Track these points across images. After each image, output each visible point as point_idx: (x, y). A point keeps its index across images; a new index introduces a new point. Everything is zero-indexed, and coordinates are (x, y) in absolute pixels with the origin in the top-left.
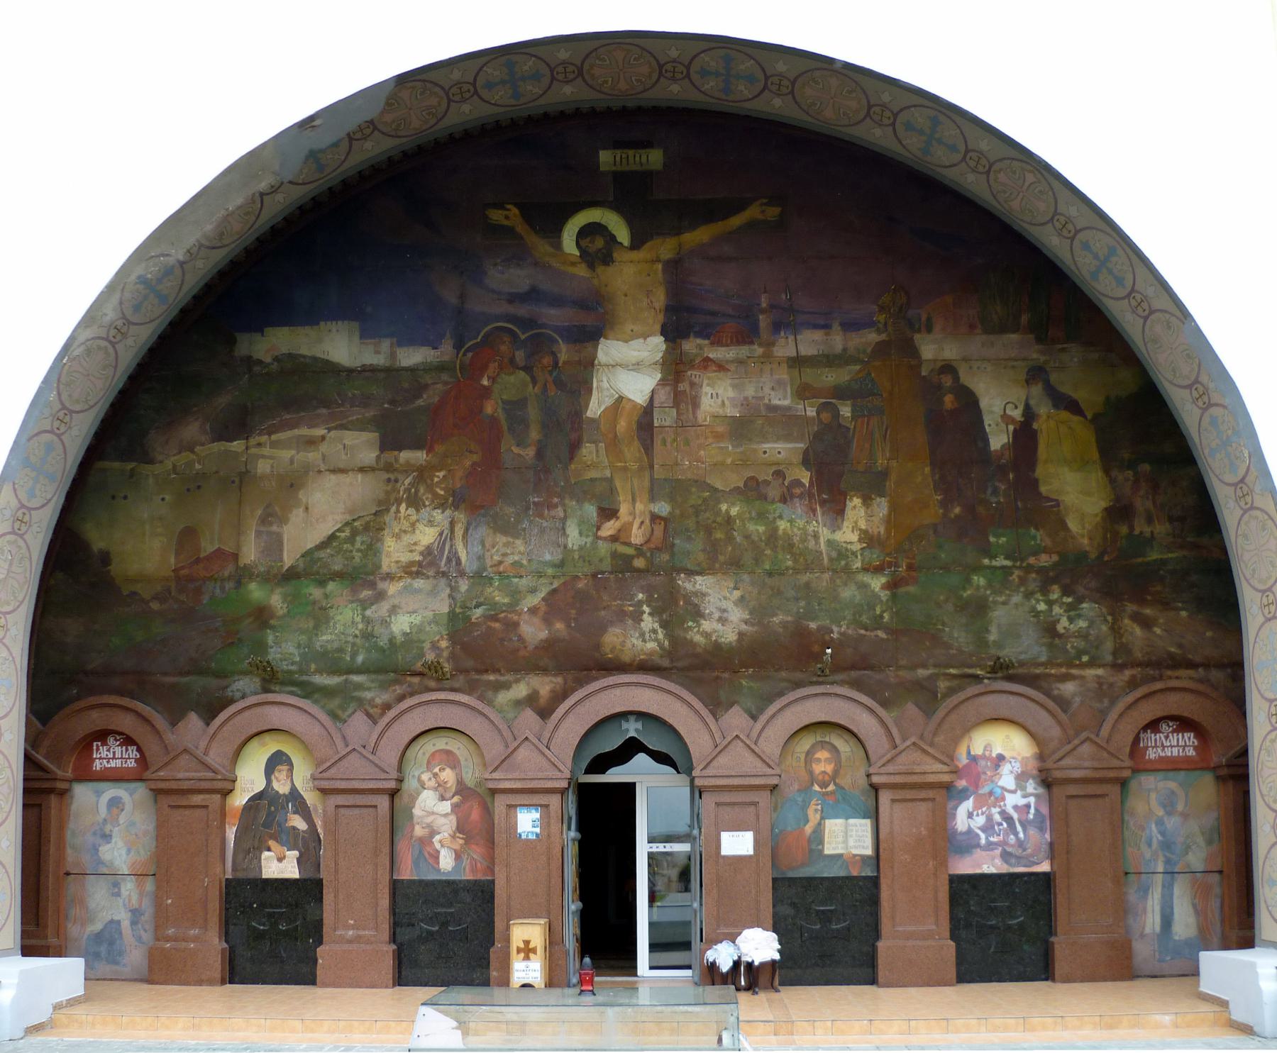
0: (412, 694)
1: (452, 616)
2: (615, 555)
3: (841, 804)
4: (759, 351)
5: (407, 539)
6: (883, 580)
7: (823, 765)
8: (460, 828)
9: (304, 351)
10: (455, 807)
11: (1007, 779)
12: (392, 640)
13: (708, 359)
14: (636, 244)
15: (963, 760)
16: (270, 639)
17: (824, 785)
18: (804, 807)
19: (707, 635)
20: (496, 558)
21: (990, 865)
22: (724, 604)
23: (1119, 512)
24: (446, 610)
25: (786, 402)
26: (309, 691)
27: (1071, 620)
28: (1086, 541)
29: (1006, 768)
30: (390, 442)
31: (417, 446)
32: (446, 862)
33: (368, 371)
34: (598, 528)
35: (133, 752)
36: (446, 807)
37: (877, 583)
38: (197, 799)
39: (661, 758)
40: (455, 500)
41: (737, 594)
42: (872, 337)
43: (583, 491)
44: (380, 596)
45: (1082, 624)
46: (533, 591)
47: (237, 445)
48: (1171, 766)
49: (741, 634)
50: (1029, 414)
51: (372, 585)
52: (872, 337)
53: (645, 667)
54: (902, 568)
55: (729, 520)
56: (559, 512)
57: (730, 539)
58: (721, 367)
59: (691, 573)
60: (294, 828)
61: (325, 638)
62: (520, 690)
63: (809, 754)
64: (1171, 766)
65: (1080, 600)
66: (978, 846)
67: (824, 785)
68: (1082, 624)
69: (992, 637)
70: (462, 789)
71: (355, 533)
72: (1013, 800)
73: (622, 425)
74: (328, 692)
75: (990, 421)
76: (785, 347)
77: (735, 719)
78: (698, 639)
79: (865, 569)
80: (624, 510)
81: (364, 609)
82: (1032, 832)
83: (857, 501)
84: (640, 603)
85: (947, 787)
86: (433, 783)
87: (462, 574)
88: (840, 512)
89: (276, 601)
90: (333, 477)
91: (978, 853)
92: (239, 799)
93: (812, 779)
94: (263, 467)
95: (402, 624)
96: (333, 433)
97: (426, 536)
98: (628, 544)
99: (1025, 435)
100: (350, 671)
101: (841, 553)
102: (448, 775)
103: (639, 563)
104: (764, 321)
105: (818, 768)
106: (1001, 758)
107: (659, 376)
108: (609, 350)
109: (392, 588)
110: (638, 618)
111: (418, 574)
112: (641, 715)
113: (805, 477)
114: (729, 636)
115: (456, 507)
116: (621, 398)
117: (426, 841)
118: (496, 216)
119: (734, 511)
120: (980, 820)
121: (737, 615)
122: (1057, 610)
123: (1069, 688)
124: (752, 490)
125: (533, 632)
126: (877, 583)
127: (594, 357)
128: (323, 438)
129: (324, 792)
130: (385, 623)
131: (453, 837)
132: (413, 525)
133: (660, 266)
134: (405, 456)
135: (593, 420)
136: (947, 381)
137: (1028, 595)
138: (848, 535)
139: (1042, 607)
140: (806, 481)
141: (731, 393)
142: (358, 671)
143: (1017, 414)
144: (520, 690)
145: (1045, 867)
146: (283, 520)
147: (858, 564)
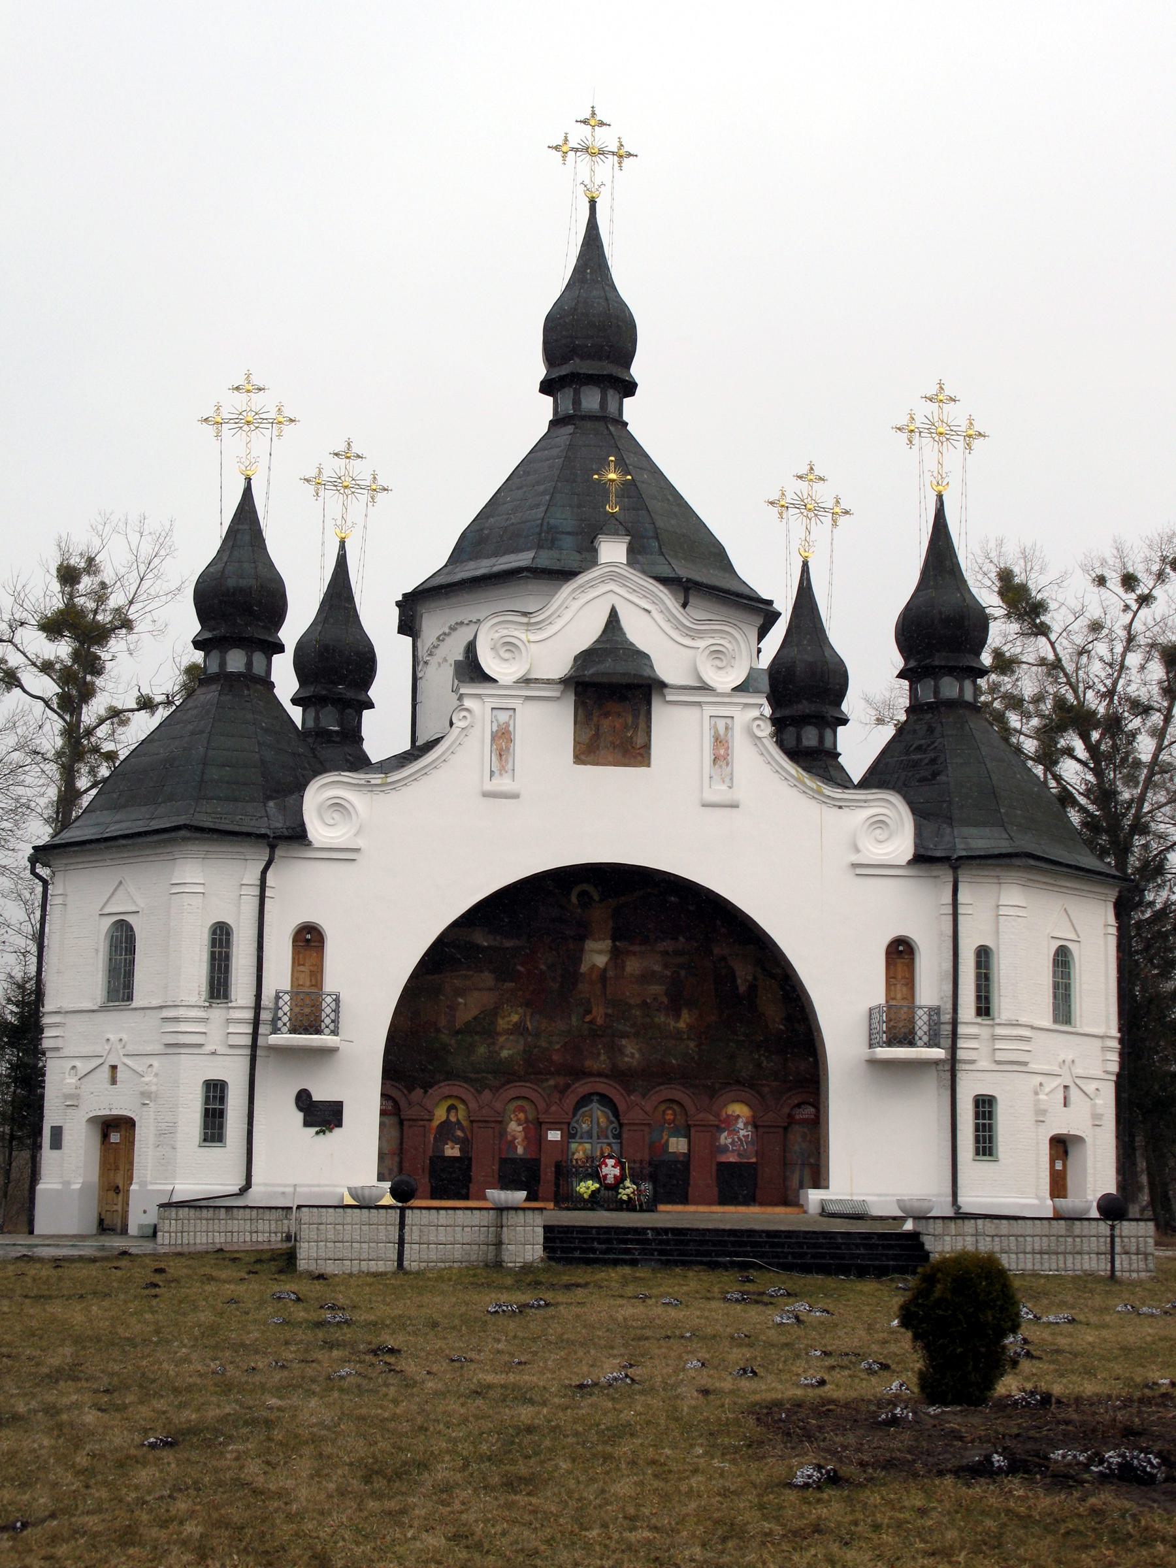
0: (509, 1083)
1: (525, 1051)
3: (676, 1133)
4: (649, 948)
5: (507, 1019)
7: (669, 1116)
8: (526, 1138)
11: (740, 1125)
14: (601, 901)
15: (724, 1115)
17: (670, 1124)
21: (732, 1159)
22: (633, 1051)
26: (467, 1080)
29: (740, 1120)
36: (520, 1128)
37: (692, 1044)
38: (421, 1123)
40: (528, 1004)
46: (558, 1043)
47: (435, 976)
50: (755, 978)
53: (600, 1074)
58: (634, 954)
62: (552, 1082)
63: (664, 1112)
66: (728, 1150)
67: (670, 1124)
70: (527, 1121)
72: (742, 1133)
73: (594, 977)
82: (750, 1146)
85: (717, 1127)
91: (729, 1154)
92: (436, 1123)
95: (505, 1053)
97: (515, 1018)
99: (753, 988)
101: (679, 1031)
102: (522, 1116)
105: (667, 1117)
106: (738, 1116)
108: (590, 945)
110: (599, 1054)
113: (665, 1000)
116: (594, 965)
119: (638, 1013)
120: (730, 1140)
122: (762, 1058)
123: (766, 1090)
126: (692, 1044)
129: (472, 1122)
130: (499, 1054)
131: (523, 1141)
135: (582, 974)
138: (682, 1025)
143: (750, 978)
144: (552, 1082)
145: (754, 1160)
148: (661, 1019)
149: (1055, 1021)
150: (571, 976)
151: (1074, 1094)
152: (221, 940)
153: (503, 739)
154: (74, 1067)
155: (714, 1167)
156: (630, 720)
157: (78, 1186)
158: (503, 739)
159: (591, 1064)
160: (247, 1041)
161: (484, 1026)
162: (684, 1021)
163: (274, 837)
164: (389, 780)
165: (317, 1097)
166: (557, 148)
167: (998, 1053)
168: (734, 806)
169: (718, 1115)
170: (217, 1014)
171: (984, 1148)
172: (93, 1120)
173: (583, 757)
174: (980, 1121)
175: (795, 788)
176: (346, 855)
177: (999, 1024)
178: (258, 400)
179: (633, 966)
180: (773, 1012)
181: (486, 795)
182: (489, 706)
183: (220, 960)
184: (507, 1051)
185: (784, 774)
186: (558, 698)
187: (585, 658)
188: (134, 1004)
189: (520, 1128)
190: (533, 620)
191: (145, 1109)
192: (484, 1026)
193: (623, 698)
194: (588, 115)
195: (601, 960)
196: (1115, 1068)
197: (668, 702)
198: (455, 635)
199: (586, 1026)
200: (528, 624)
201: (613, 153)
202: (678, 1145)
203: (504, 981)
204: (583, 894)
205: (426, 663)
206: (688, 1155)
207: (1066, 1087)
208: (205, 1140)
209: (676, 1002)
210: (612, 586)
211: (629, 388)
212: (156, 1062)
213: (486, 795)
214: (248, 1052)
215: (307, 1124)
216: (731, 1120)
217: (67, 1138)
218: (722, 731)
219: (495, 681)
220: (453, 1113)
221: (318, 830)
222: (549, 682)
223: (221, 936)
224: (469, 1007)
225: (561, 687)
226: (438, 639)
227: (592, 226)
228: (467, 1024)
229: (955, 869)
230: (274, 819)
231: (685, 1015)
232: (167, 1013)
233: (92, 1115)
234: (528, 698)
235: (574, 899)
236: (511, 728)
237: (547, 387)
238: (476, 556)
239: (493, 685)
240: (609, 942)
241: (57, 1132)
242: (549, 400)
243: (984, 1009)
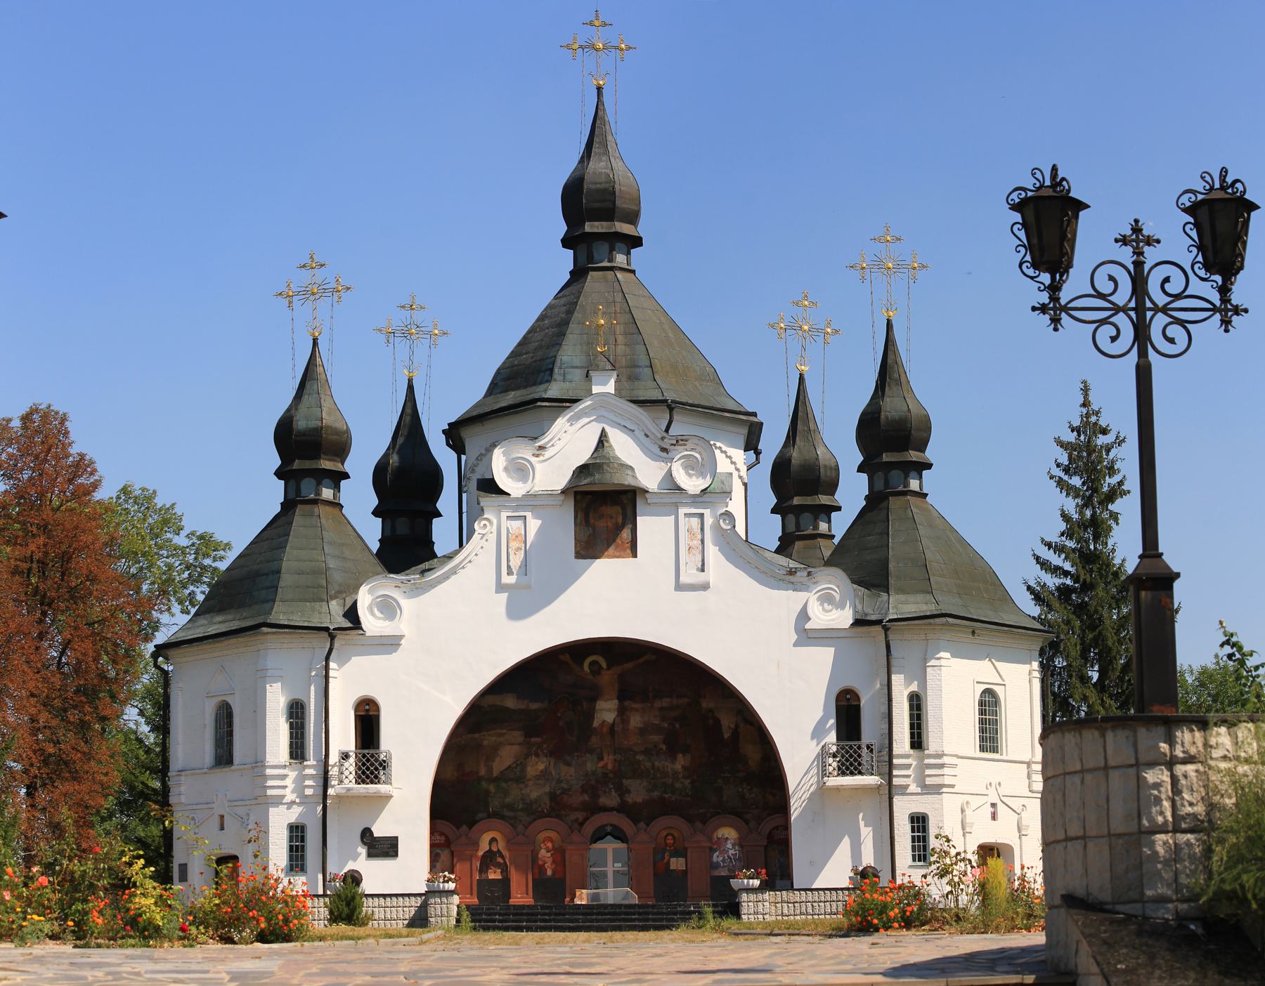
4: (649, 705)
6: (689, 781)
8: (554, 862)
9: (498, 704)
10: (552, 855)
14: (608, 669)
16: (490, 800)
25: (657, 722)
26: (502, 817)
29: (729, 842)
35: (443, 838)
36: (549, 854)
37: (687, 782)
39: (616, 838)
42: (686, 700)
43: (591, 751)
44: (526, 786)
45: (753, 795)
47: (477, 735)
50: (737, 726)
52: (686, 700)
53: (612, 809)
54: (695, 777)
58: (637, 710)
59: (627, 779)
61: (508, 800)
71: (517, 765)
72: (731, 852)
73: (605, 729)
75: (724, 729)
76: (658, 704)
77: (642, 825)
80: (605, 758)
83: (681, 755)
84: (611, 789)
88: (676, 759)
89: (492, 788)
90: (509, 747)
92: (481, 853)
93: (666, 845)
94: (485, 743)
95: (534, 795)
97: (541, 767)
99: (735, 733)
102: (550, 845)
106: (727, 838)
107: (616, 713)
108: (601, 704)
109: (531, 783)
111: (538, 779)
112: (611, 825)
113: (664, 747)
114: (639, 800)
115: (551, 756)
116: (604, 721)
118: (561, 657)
124: (647, 752)
134: (533, 740)
135: (595, 728)
143: (733, 726)
146: (494, 761)
147: (681, 776)
149: (982, 749)
151: (1001, 809)
152: (297, 713)
156: (620, 520)
159: (604, 800)
161: (516, 775)
162: (680, 762)
163: (334, 629)
165: (377, 833)
168: (705, 587)
169: (710, 838)
171: (919, 855)
173: (583, 552)
174: (916, 834)
177: (930, 756)
178: (320, 275)
179: (636, 721)
180: (752, 754)
183: (297, 728)
184: (535, 793)
189: (549, 854)
192: (516, 775)
195: (610, 717)
196: (1039, 786)
202: (677, 864)
203: (664, 743)
204: (593, 663)
206: (685, 872)
207: (993, 805)
208: (291, 870)
211: (637, 242)
219: (509, 495)
221: (372, 623)
222: (550, 495)
224: (506, 757)
225: (562, 497)
226: (477, 459)
228: (501, 772)
229: (886, 629)
230: (334, 614)
237: (567, 242)
238: (506, 391)
240: (616, 701)
241: (183, 868)
242: (570, 253)
243: (917, 742)
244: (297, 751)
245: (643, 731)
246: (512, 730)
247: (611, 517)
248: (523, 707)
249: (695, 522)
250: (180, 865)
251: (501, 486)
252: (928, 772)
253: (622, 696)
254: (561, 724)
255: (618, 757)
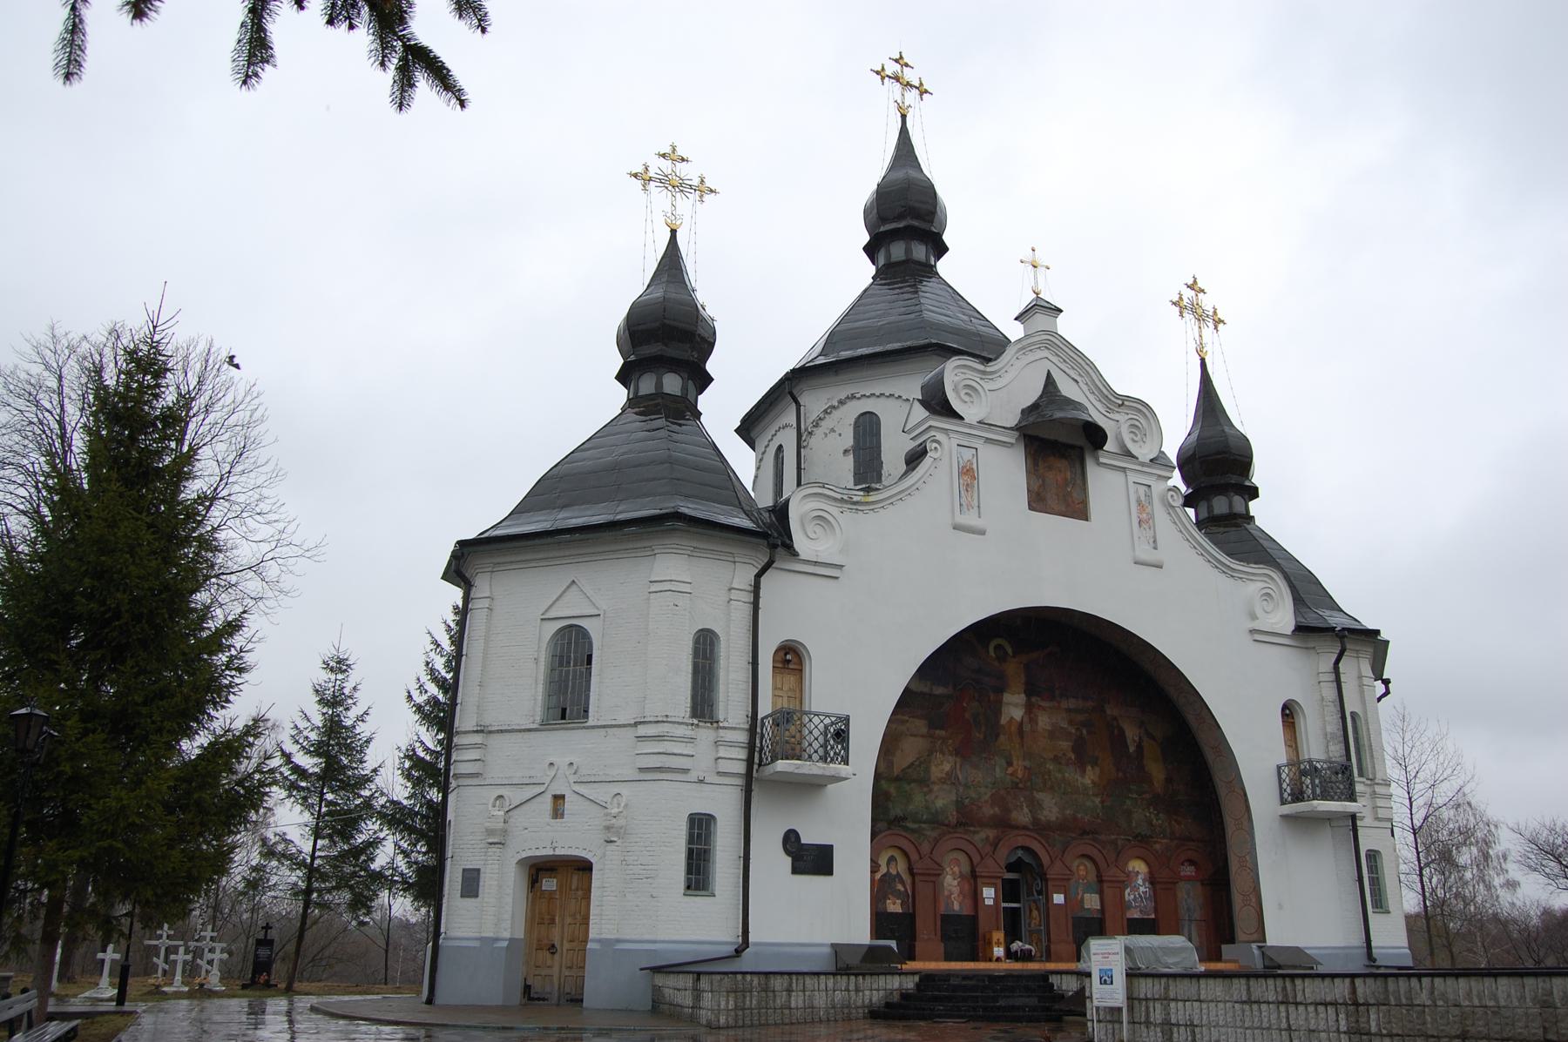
1: (957, 801)
2: (1013, 782)
3: (1088, 890)
8: (961, 892)
10: (959, 883)
12: (936, 811)
13: (1040, 706)
16: (891, 805)
18: (1077, 888)
19: (1046, 817)
20: (972, 779)
21: (1137, 915)
23: (1169, 780)
24: (955, 799)
27: (1157, 820)
28: (1159, 790)
29: (1140, 877)
30: (932, 725)
31: (942, 728)
32: (956, 907)
33: (923, 694)
34: (1007, 770)
36: (956, 883)
37: (1097, 800)
40: (957, 753)
41: (1054, 801)
46: (986, 794)
48: (1188, 879)
49: (1057, 818)
51: (928, 786)
53: (1025, 828)
55: (1050, 771)
56: (993, 762)
57: (1050, 779)
58: (1044, 709)
60: (899, 890)
63: (1078, 866)
64: (1188, 879)
65: (1159, 813)
68: (1160, 822)
69: (1134, 825)
72: (1142, 889)
74: (913, 831)
76: (1064, 704)
78: (1043, 818)
79: (1093, 795)
80: (1015, 763)
81: (925, 796)
82: (1149, 902)
86: (951, 873)
87: (960, 784)
88: (1085, 771)
89: (893, 791)
90: (912, 738)
95: (939, 803)
96: (911, 719)
97: (947, 767)
98: (1017, 778)
99: (1139, 747)
100: (921, 822)
102: (956, 869)
103: (1020, 785)
104: (1057, 692)
105: (1081, 873)
108: (1007, 697)
109: (936, 788)
111: (944, 783)
115: (956, 755)
117: (949, 897)
119: (1051, 767)
120: (1132, 897)
121: (1055, 810)
122: (1153, 816)
124: (1056, 759)
125: (989, 811)
127: (1002, 699)
128: (907, 721)
132: (942, 761)
133: (1022, 666)
134: (937, 732)
136: (1115, 723)
137: (1143, 810)
139: (1148, 814)
140: (1073, 757)
141: (1048, 720)
142: (924, 823)
143: (1137, 739)
144: (982, 835)
145: (1153, 916)
148: (1071, 774)
150: (994, 728)
152: (705, 651)
153: (968, 473)
154: (501, 797)
155: (1125, 923)
157: (505, 944)
158: (968, 473)
160: (741, 768)
162: (1089, 777)
164: (871, 499)
166: (878, 73)
167: (1379, 810)
170: (705, 734)
172: (521, 862)
173: (1034, 505)
174: (1375, 876)
175: (1201, 557)
176: (828, 571)
179: (1044, 721)
181: (956, 527)
182: (955, 442)
184: (943, 800)
185: (1193, 542)
186: (1012, 444)
187: (1027, 412)
188: (591, 722)
190: (988, 369)
191: (611, 847)
193: (1063, 456)
194: (879, 69)
197: (1099, 464)
198: (844, 409)
199: (1008, 777)
200: (984, 373)
201: (916, 87)
204: (998, 647)
205: (810, 433)
208: (688, 887)
209: (1082, 758)
210: (1046, 353)
212: (625, 790)
213: (956, 527)
214: (740, 781)
215: (795, 871)
216: (1129, 877)
217: (488, 883)
218: (1143, 498)
219: (962, 418)
220: (893, 865)
223: (705, 646)
225: (1016, 434)
227: (904, 133)
228: (902, 770)
231: (1089, 768)
232: (642, 731)
233: (524, 855)
234: (988, 440)
235: (992, 653)
236: (975, 466)
239: (959, 422)
244: (703, 706)
245: (1053, 734)
246: (913, 717)
247: (1060, 471)
248: (926, 690)
249: (1142, 490)
250: (464, 870)
251: (956, 404)
252: (1380, 803)
253: (1031, 691)
254: (967, 715)
255: (1027, 763)
